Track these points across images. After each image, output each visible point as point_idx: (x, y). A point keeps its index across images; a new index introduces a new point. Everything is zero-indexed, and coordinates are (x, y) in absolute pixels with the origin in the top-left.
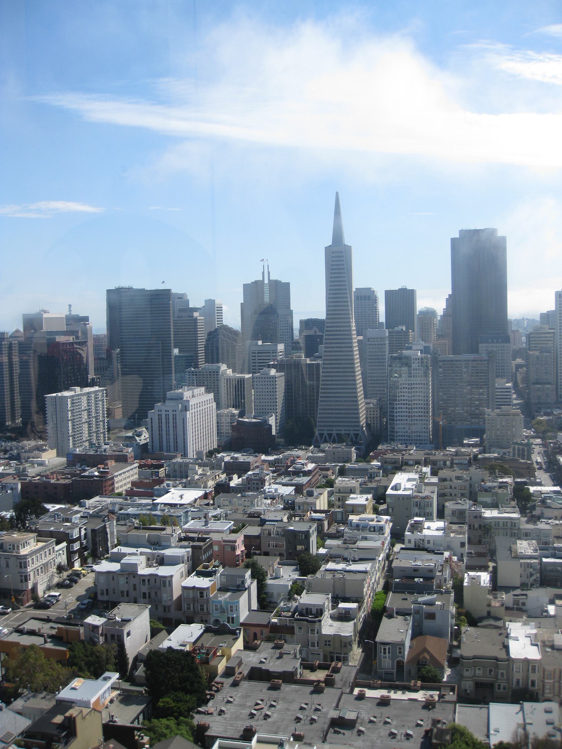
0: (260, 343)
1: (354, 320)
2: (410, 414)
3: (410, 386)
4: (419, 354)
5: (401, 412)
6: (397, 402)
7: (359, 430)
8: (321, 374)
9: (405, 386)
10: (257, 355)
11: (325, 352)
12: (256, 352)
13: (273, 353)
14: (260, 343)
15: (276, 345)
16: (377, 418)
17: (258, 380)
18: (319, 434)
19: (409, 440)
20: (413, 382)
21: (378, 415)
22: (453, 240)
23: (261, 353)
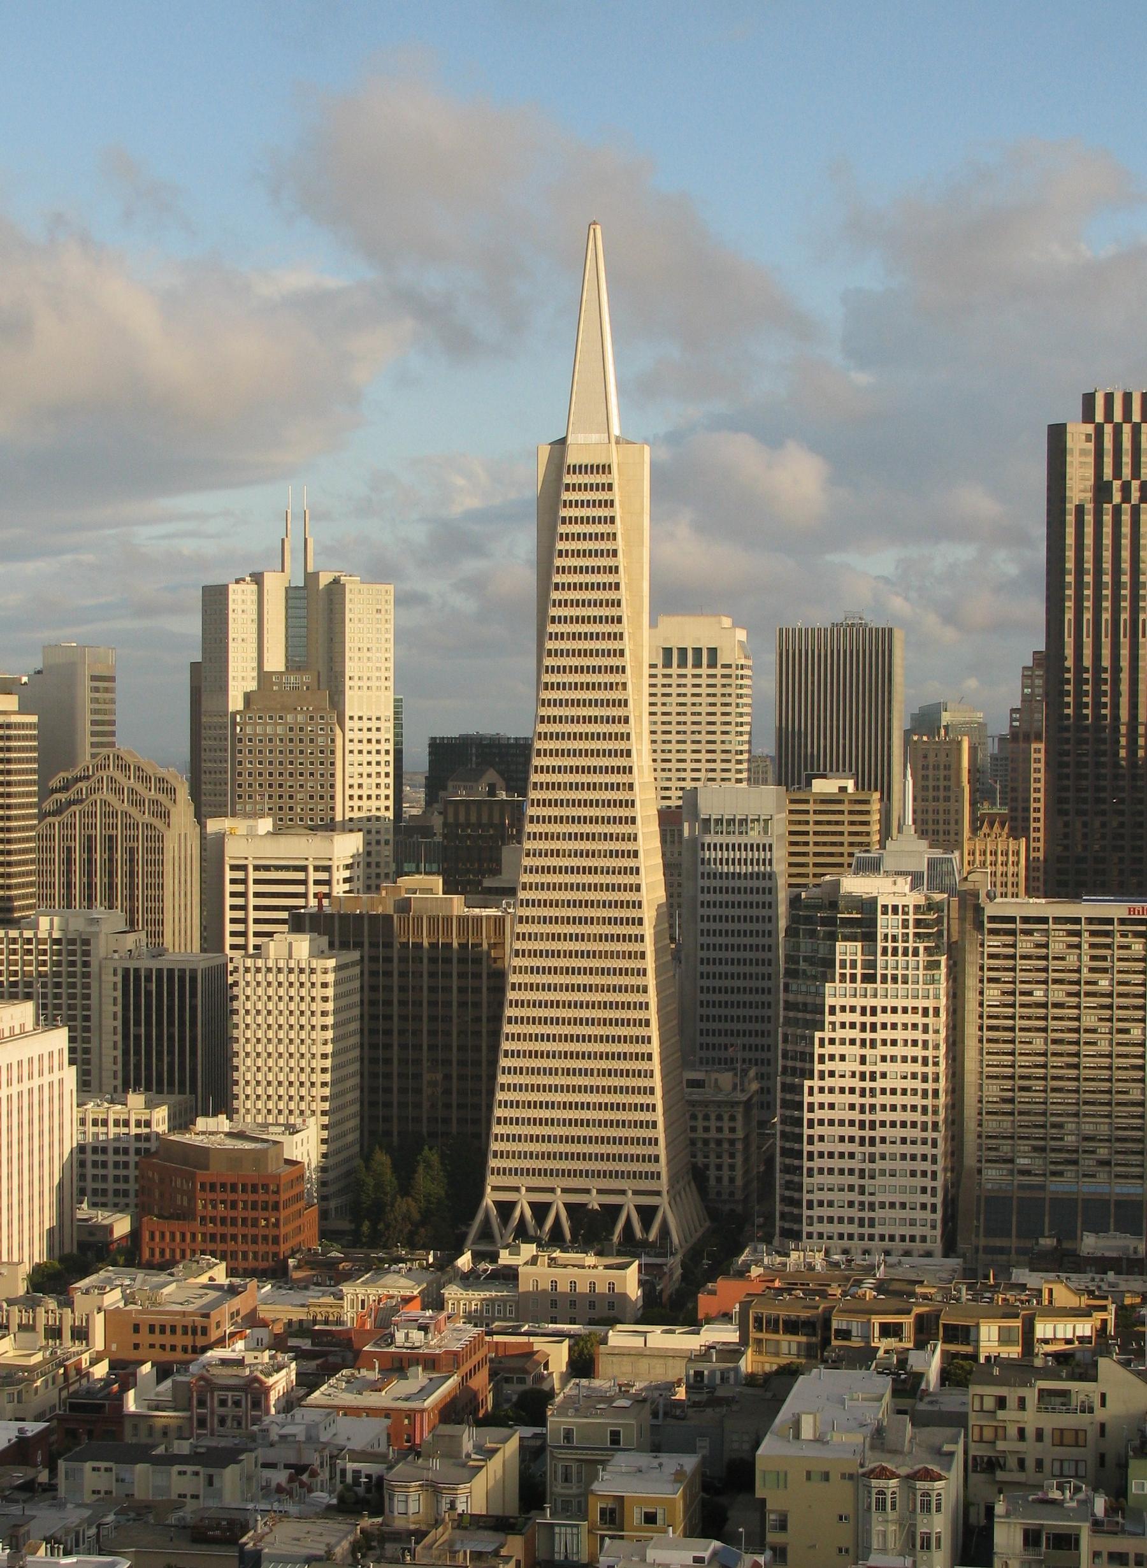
7: (658, 1193)
9: (848, 1017)
16: (732, 1142)
18: (498, 1204)
19: (861, 1237)
20: (879, 1002)
21: (740, 1134)
23: (267, 868)
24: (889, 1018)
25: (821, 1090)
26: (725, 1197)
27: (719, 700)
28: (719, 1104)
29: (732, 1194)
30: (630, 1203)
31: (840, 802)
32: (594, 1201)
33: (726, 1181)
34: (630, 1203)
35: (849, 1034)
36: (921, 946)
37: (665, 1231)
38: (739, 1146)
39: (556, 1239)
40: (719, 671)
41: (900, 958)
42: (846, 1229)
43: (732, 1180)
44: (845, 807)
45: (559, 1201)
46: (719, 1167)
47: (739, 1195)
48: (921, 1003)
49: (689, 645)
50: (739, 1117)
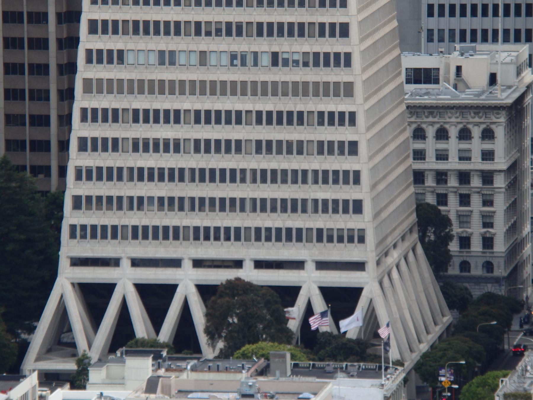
7: (359, 266)
16: (487, 177)
21: (501, 163)
26: (477, 271)
28: (462, 109)
29: (489, 266)
30: (310, 283)
34: (310, 283)
38: (500, 182)
43: (488, 242)
45: (187, 282)
50: (500, 132)
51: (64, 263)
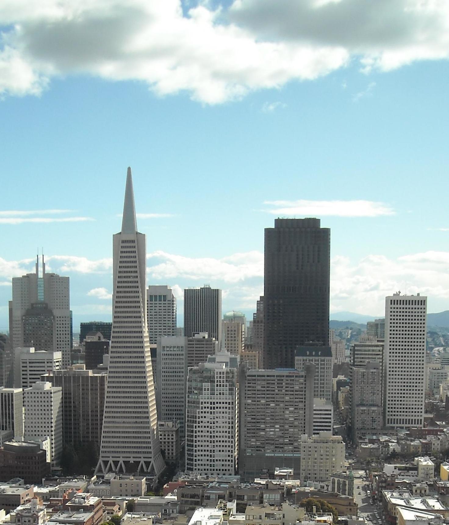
0: (32, 350)
1: (146, 325)
2: (212, 439)
3: (213, 406)
4: (224, 367)
5: (202, 436)
6: (197, 425)
7: (151, 458)
8: (106, 389)
9: (206, 405)
10: (28, 365)
11: (111, 362)
12: (28, 361)
13: (47, 362)
14: (32, 350)
15: (52, 354)
16: (172, 442)
17: (30, 395)
18: (104, 461)
19: (211, 470)
20: (216, 401)
21: (174, 440)
22: (268, 231)
23: (33, 363)
24: (218, 405)
25: (199, 427)
26: (170, 458)
27: (167, 311)
28: (168, 431)
29: (172, 458)
30: (142, 461)
31: (203, 341)
32: (132, 460)
33: (171, 454)
34: (142, 461)
35: (206, 410)
36: (228, 384)
37: (153, 469)
38: (174, 443)
39: (121, 471)
40: (167, 302)
41: (222, 387)
42: (206, 467)
43: (172, 453)
44: (204, 343)
45: (121, 460)
46: (169, 450)
47: (174, 458)
48: (228, 401)
49: (158, 294)
50: (174, 435)
51: (100, 457)
